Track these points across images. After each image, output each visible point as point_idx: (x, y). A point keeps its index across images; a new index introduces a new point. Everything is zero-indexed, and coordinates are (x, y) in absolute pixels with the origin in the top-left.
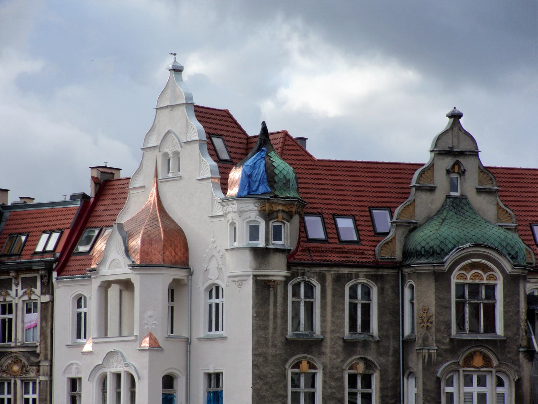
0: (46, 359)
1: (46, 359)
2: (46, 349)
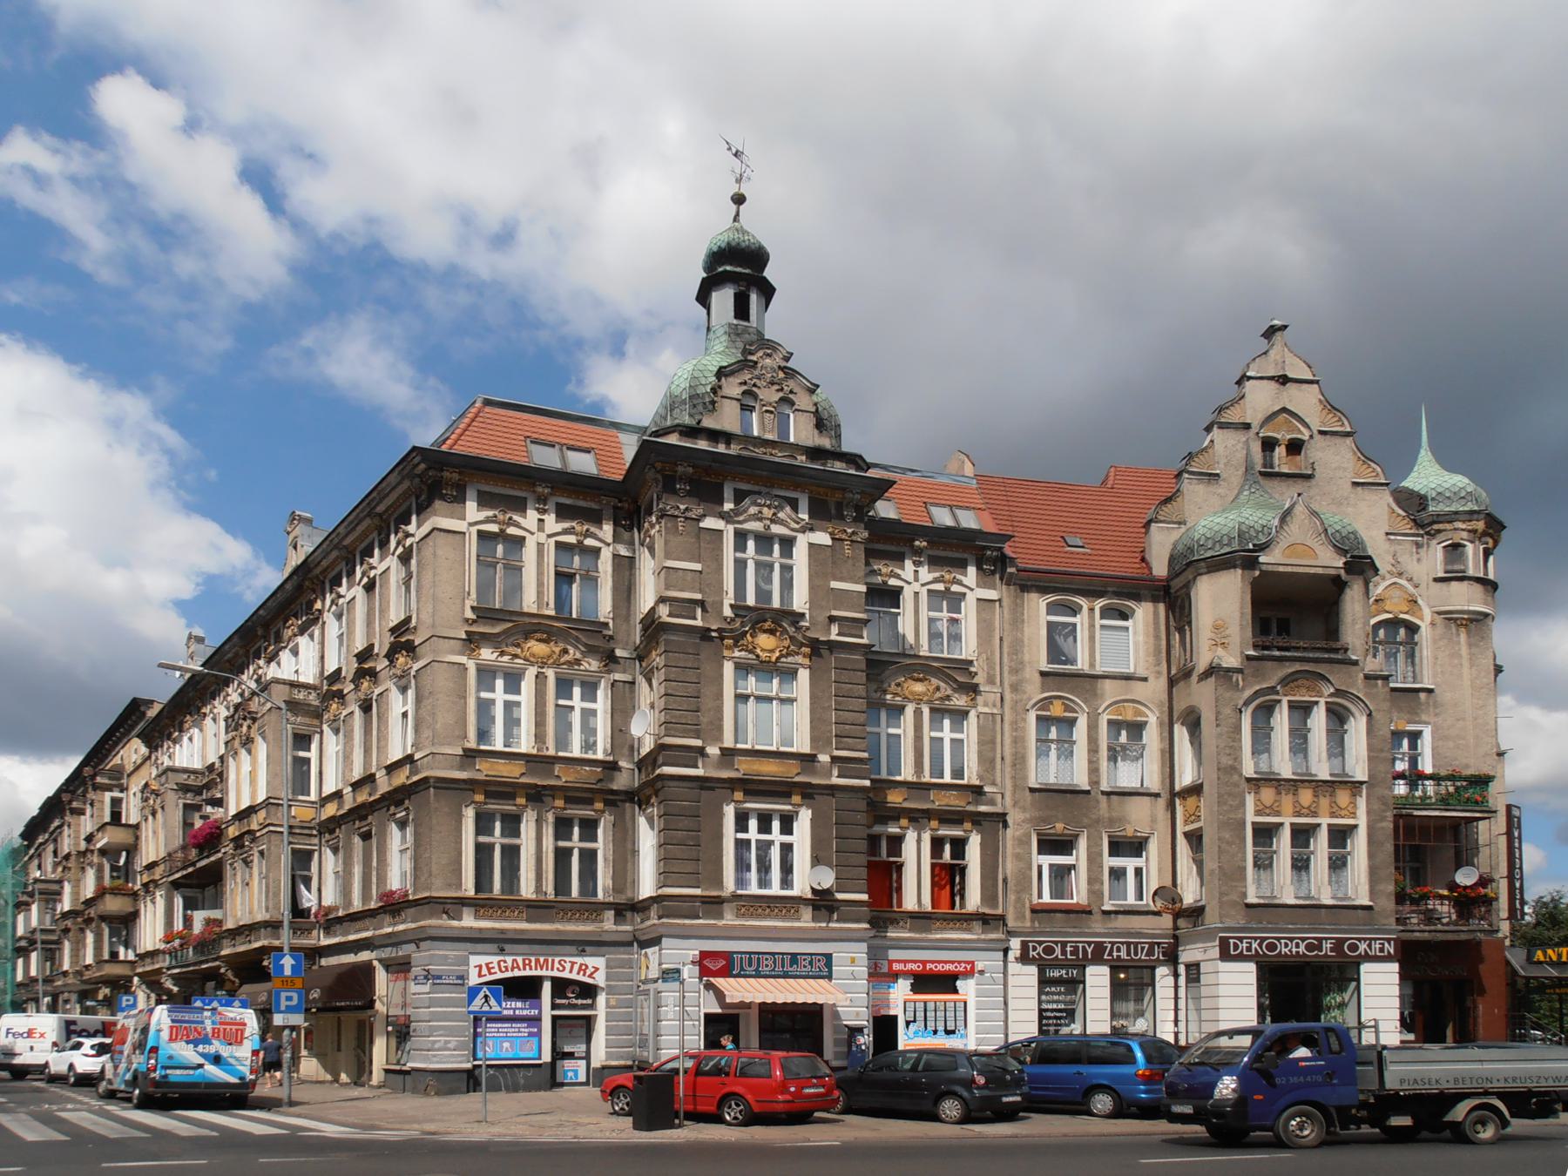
0: (991, 681)
1: (991, 681)
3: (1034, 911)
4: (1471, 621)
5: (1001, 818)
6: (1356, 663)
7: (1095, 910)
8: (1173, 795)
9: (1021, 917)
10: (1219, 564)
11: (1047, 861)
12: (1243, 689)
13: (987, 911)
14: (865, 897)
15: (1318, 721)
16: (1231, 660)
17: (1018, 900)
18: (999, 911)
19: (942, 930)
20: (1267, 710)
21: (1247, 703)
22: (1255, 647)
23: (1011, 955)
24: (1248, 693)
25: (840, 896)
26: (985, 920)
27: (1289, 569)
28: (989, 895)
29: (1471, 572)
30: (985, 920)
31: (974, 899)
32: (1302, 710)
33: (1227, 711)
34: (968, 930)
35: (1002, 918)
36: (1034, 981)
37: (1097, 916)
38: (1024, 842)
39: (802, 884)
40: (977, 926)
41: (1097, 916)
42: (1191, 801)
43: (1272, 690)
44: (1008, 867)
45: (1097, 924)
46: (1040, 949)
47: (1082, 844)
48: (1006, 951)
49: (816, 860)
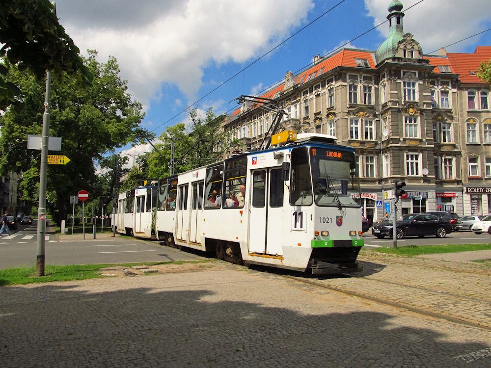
2: (456, 111)
5: (459, 153)
7: (483, 179)
9: (465, 181)
11: (472, 164)
14: (434, 176)
17: (465, 176)
18: (460, 179)
19: (448, 185)
23: (464, 192)
25: (428, 176)
26: (458, 182)
28: (458, 175)
30: (458, 182)
34: (454, 185)
35: (461, 181)
36: (469, 199)
37: (484, 180)
38: (465, 159)
39: (420, 174)
41: (484, 180)
44: (462, 166)
46: (471, 190)
47: (479, 160)
48: (463, 191)
49: (424, 167)
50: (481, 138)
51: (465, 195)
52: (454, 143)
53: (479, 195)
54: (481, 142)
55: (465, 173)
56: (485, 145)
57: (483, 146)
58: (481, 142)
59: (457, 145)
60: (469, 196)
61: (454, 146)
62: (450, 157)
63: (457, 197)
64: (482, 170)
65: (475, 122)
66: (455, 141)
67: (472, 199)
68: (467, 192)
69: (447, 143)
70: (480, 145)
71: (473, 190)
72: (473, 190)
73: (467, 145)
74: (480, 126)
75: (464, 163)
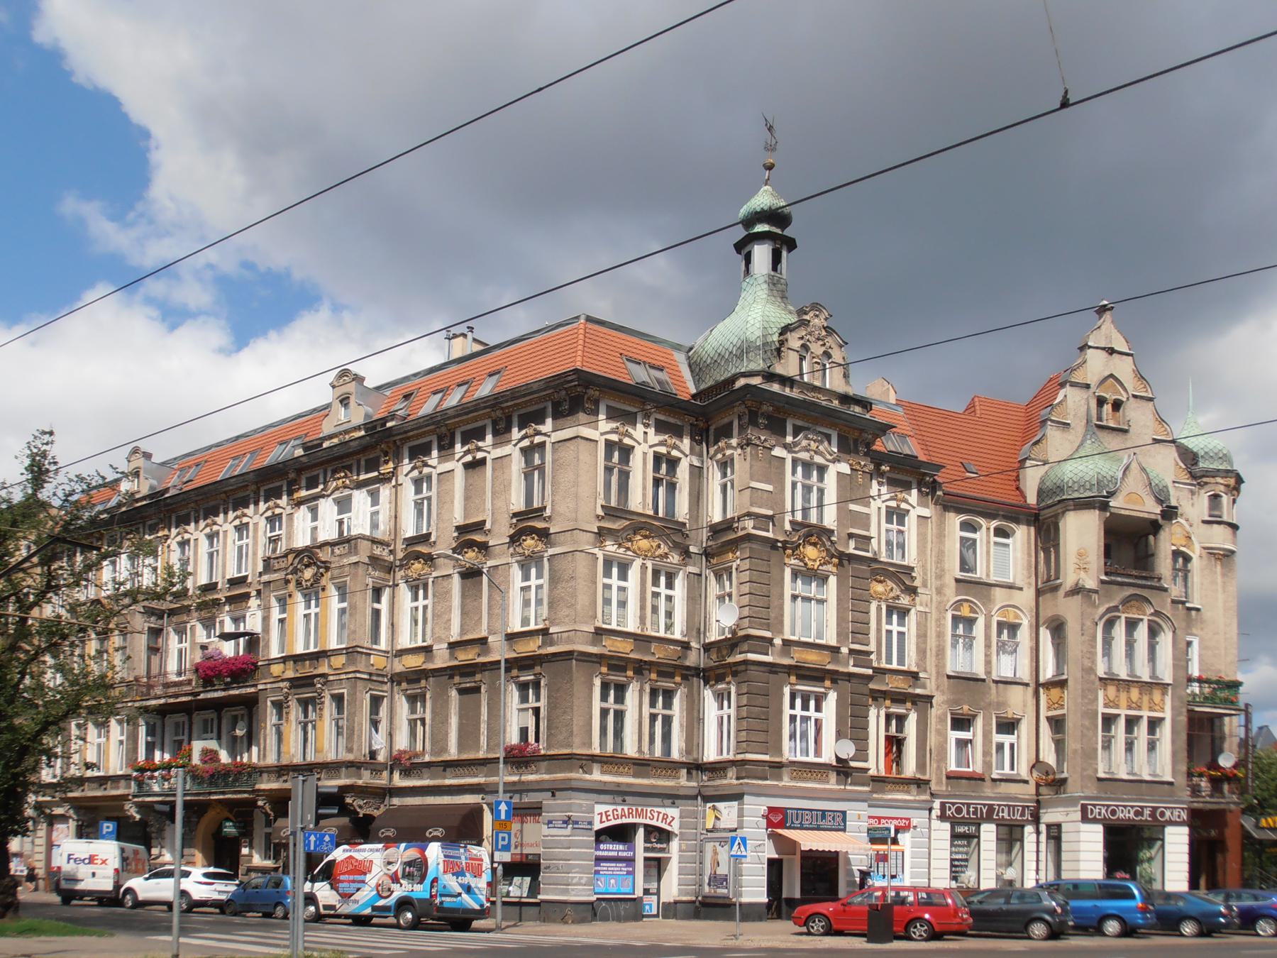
3: (948, 777)
4: (1224, 556)
6: (1166, 590)
7: (987, 778)
8: (1038, 685)
9: (939, 782)
10: (1083, 504)
11: (954, 735)
12: (1097, 607)
13: (918, 776)
15: (1142, 632)
16: (1091, 583)
17: (939, 768)
18: (927, 777)
19: (891, 791)
20: (1110, 624)
21: (1101, 619)
22: (1106, 574)
24: (1102, 610)
25: (853, 764)
26: (920, 784)
27: (1127, 513)
28: (921, 765)
29: (1225, 518)
30: (920, 784)
31: (910, 767)
32: (1132, 625)
33: (1088, 623)
34: (908, 792)
35: (927, 782)
37: (988, 783)
38: (942, 720)
39: (827, 757)
40: (913, 788)
41: (988, 783)
42: (1055, 692)
43: (1116, 608)
44: (932, 740)
45: (988, 790)
46: (953, 809)
47: (979, 722)
48: (930, 810)
49: (839, 735)
50: (988, 663)
51: (936, 824)
52: (915, 669)
53: (973, 824)
54: (988, 673)
55: (938, 761)
56: (996, 682)
57: (993, 686)
58: (988, 673)
59: (921, 675)
60: (947, 826)
61: (914, 676)
62: (901, 711)
63: (915, 827)
64: (986, 753)
65: (976, 612)
66: (918, 665)
67: (955, 836)
68: (943, 817)
69: (894, 666)
70: (983, 680)
71: (959, 810)
72: (959, 810)
73: (949, 677)
74: (988, 627)
75: (938, 732)
